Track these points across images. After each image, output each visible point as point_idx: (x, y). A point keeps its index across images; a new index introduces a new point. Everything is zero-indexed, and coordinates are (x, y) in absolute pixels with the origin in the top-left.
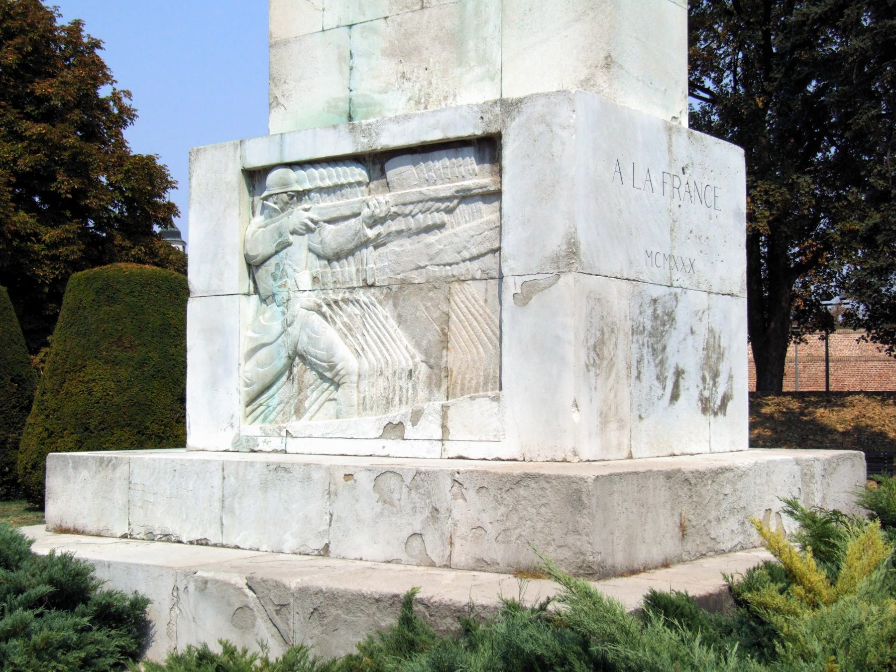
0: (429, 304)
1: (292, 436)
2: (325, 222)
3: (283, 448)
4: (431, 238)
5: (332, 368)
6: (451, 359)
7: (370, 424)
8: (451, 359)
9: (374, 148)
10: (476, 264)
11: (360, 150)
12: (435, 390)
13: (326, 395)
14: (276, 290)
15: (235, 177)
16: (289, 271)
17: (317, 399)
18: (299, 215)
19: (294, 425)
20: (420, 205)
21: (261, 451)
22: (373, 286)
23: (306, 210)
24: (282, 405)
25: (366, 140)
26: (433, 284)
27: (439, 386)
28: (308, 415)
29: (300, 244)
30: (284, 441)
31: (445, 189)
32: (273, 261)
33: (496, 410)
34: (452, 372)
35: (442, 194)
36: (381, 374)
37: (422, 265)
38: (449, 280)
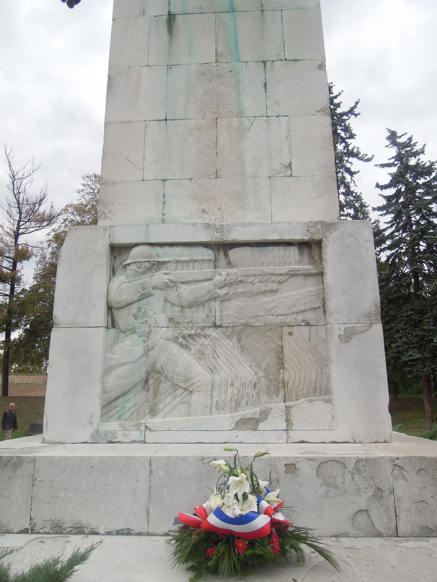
0: (267, 340)
1: (150, 430)
2: (180, 283)
3: (142, 438)
5: (187, 380)
6: (286, 375)
7: (226, 419)
8: (285, 375)
9: (225, 239)
10: (300, 317)
11: (214, 240)
12: (274, 396)
13: (178, 399)
14: (137, 325)
15: (103, 248)
16: (150, 313)
17: (171, 402)
18: (159, 277)
19: (150, 421)
20: (260, 277)
21: (120, 442)
22: (220, 326)
23: (166, 274)
24: (137, 407)
25: (219, 234)
26: (269, 327)
27: (277, 394)
28: (161, 414)
29: (159, 295)
30: (143, 434)
31: (283, 269)
32: (135, 307)
33: (330, 409)
34: (288, 383)
35: (278, 272)
36: (232, 384)
37: (261, 314)
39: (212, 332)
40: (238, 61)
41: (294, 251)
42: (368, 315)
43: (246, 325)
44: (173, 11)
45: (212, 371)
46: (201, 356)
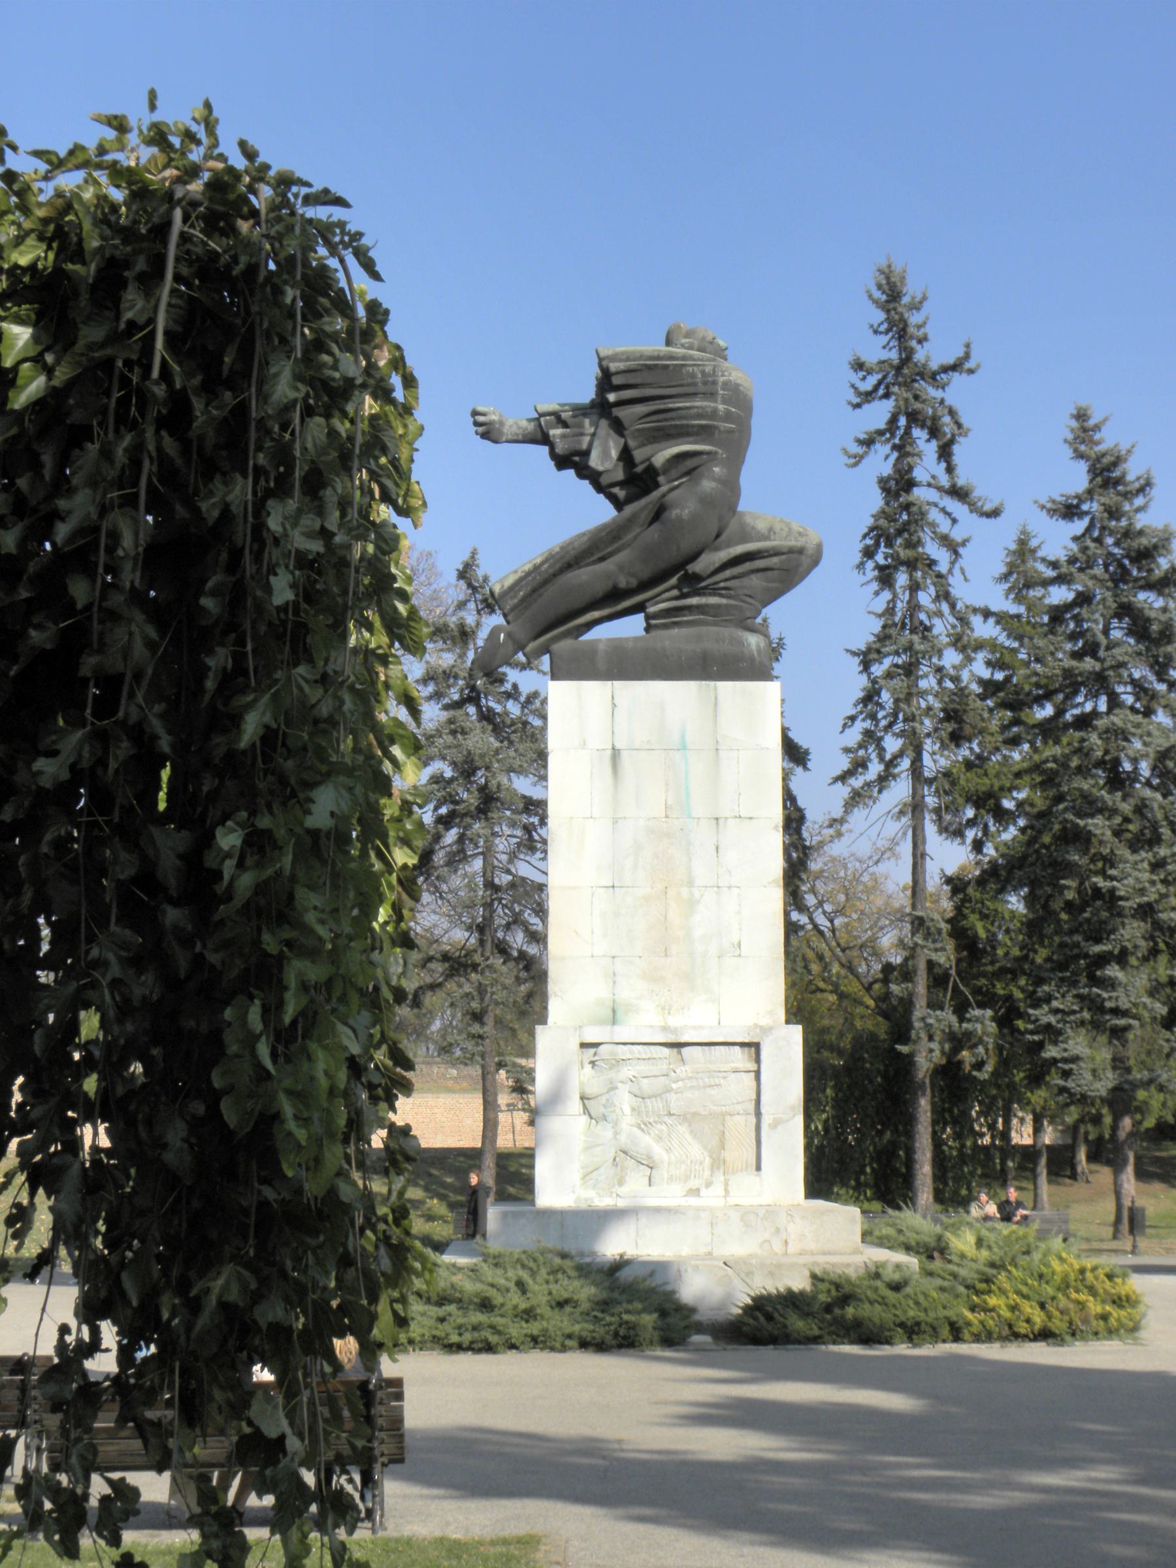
4: (713, 1092)
5: (649, 1157)
38: (723, 1115)
39: (666, 1119)
40: (690, 817)
41: (737, 1048)
42: (792, 1108)
43: (695, 1114)
44: (618, 746)
45: (668, 1150)
46: (659, 1139)
